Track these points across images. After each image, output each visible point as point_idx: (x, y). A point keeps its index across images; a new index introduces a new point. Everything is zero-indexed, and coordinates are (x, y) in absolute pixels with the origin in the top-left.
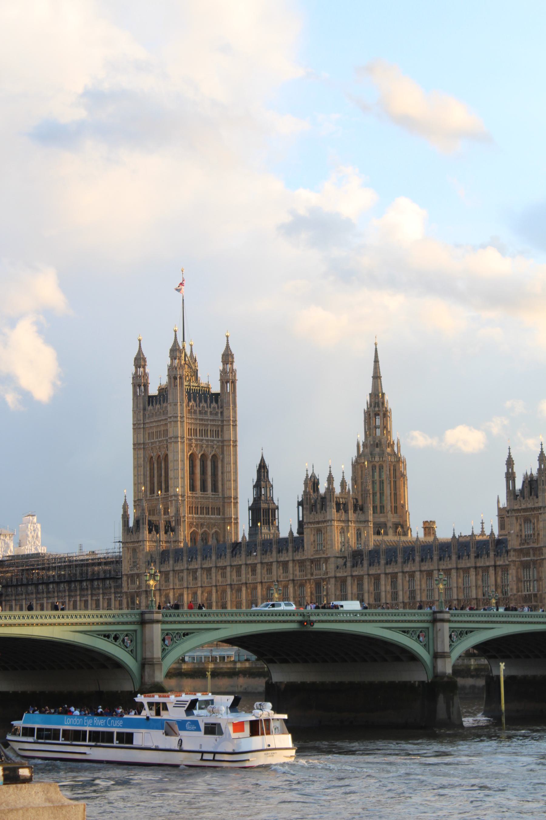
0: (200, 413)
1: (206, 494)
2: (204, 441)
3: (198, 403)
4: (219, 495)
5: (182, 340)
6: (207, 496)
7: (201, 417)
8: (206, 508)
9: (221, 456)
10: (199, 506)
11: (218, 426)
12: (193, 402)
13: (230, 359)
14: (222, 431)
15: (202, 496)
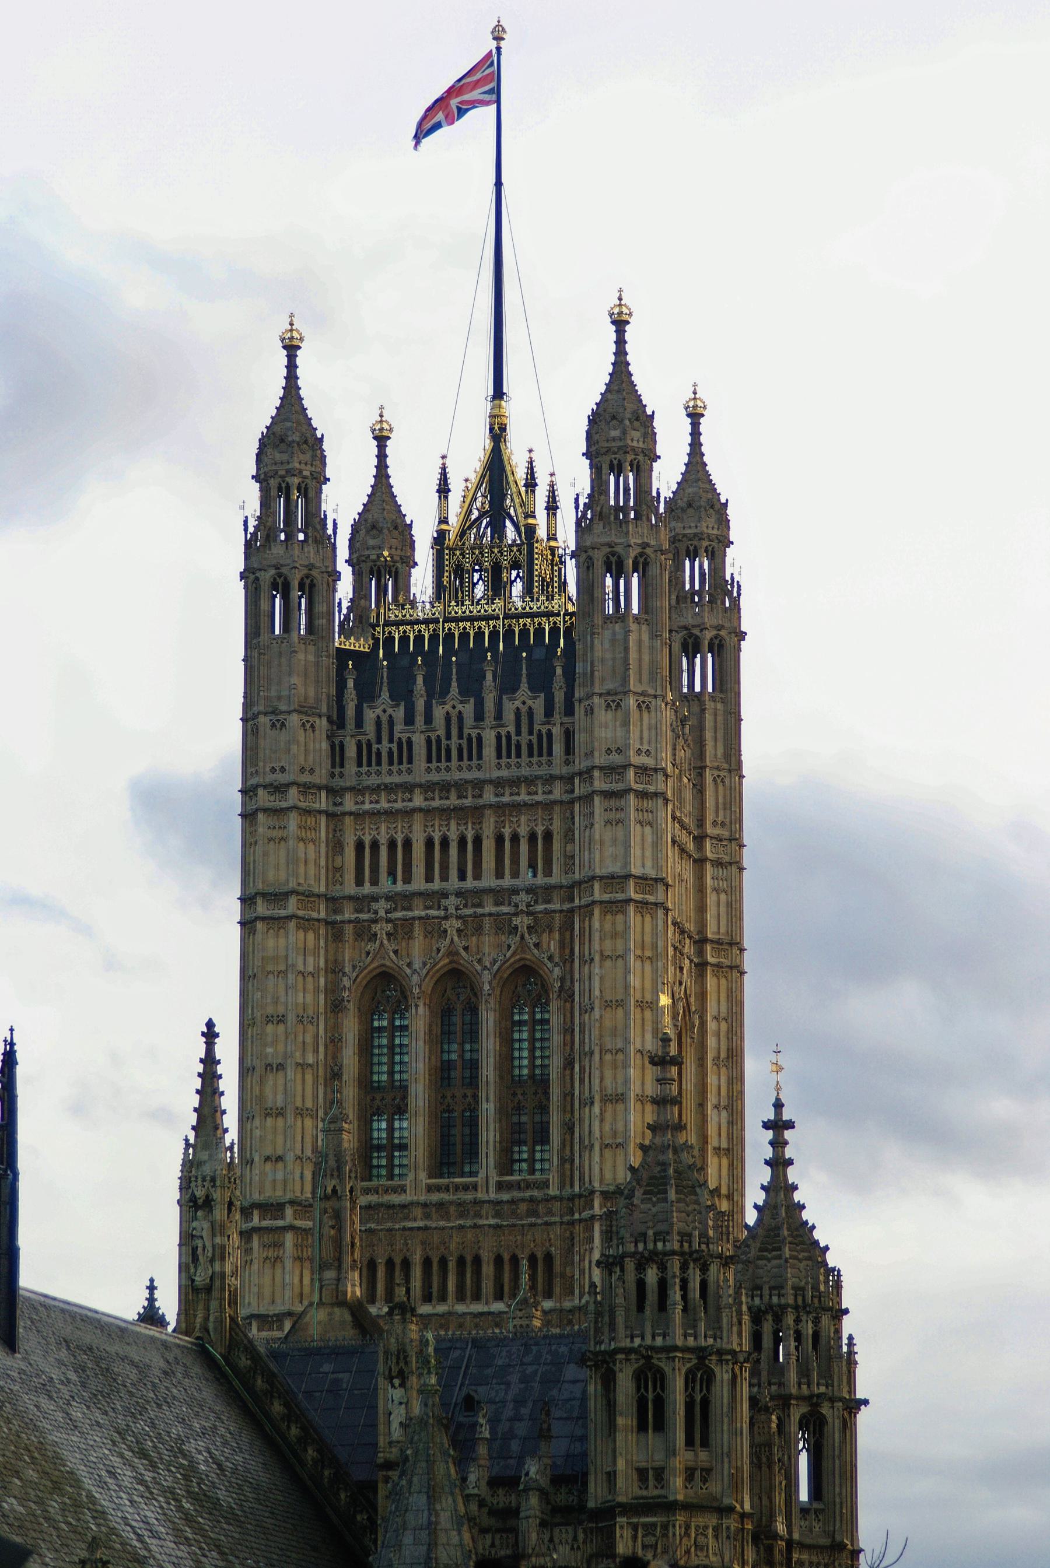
0: (436, 751)
1: (466, 1188)
2: (452, 901)
3: (420, 705)
4: (546, 1184)
5: (491, 392)
6: (469, 1196)
7: (435, 777)
8: (461, 1262)
9: (557, 971)
10: (417, 1258)
11: (548, 806)
12: (385, 695)
13: (635, 439)
14: (569, 836)
15: (435, 1197)
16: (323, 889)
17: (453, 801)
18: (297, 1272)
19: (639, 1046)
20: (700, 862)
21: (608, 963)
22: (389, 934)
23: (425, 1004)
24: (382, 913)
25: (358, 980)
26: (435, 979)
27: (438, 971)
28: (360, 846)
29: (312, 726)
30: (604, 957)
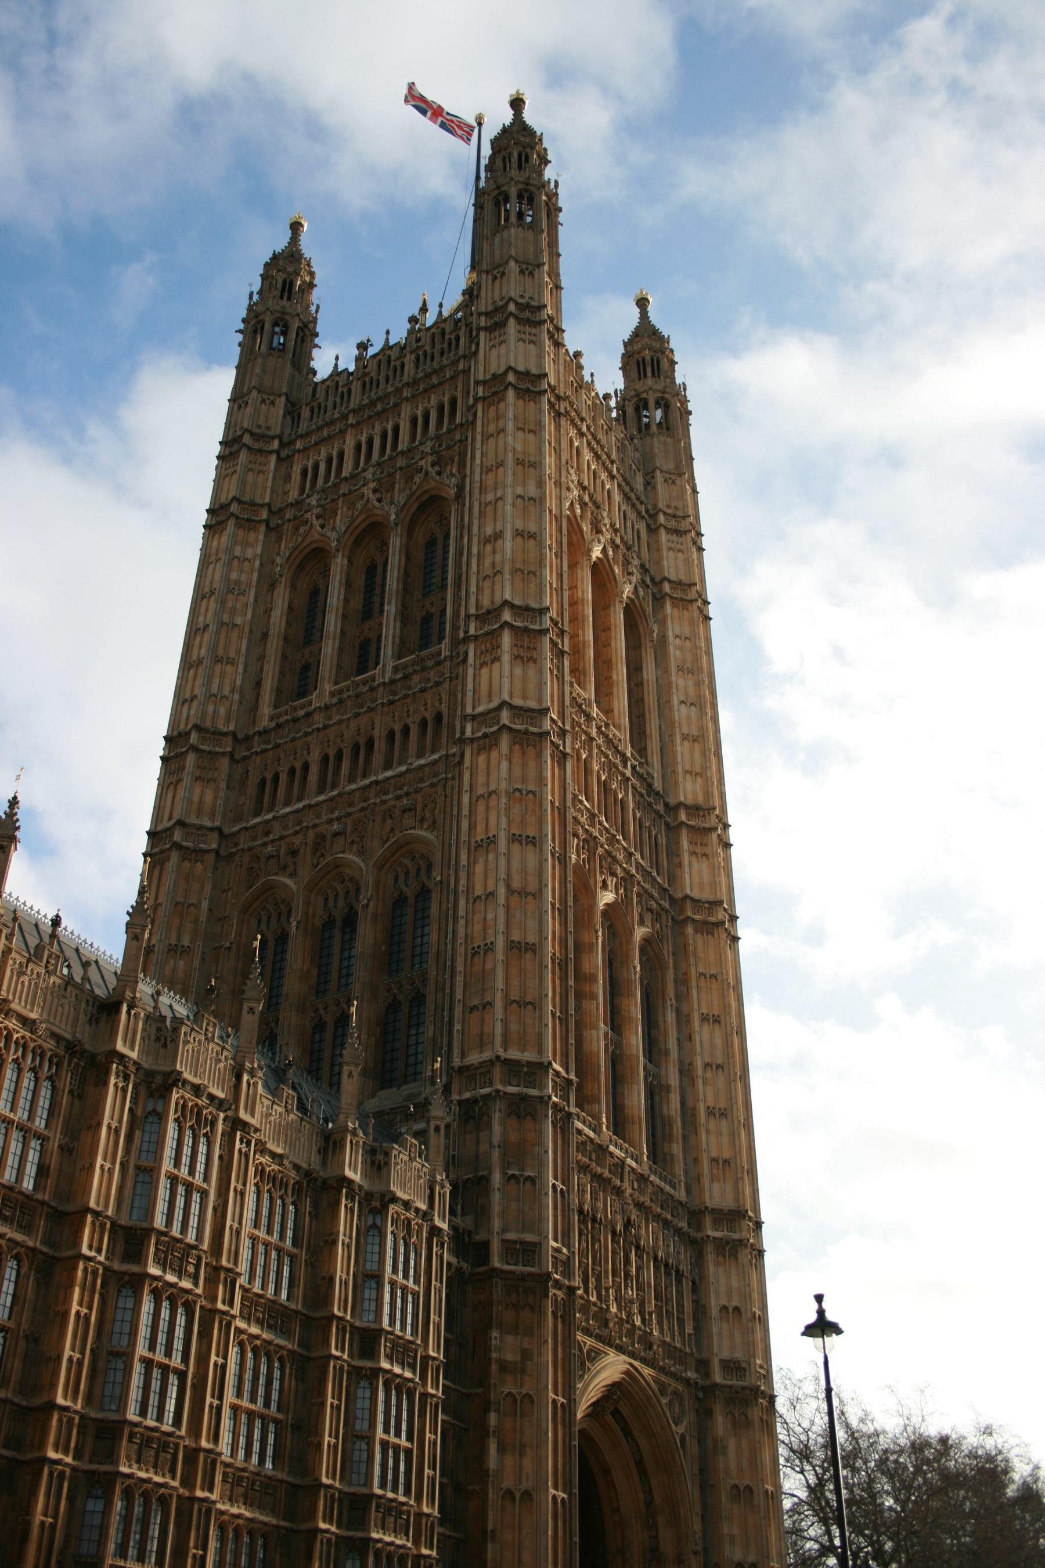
8: (356, 748)
10: (315, 756)
16: (267, 500)
17: (379, 407)
18: (197, 791)
19: (519, 491)
20: (652, 530)
21: (491, 440)
22: (318, 517)
23: (343, 556)
24: (314, 502)
25: (292, 558)
26: (355, 535)
27: (357, 527)
28: (304, 472)
29: (273, 403)
30: (486, 437)
